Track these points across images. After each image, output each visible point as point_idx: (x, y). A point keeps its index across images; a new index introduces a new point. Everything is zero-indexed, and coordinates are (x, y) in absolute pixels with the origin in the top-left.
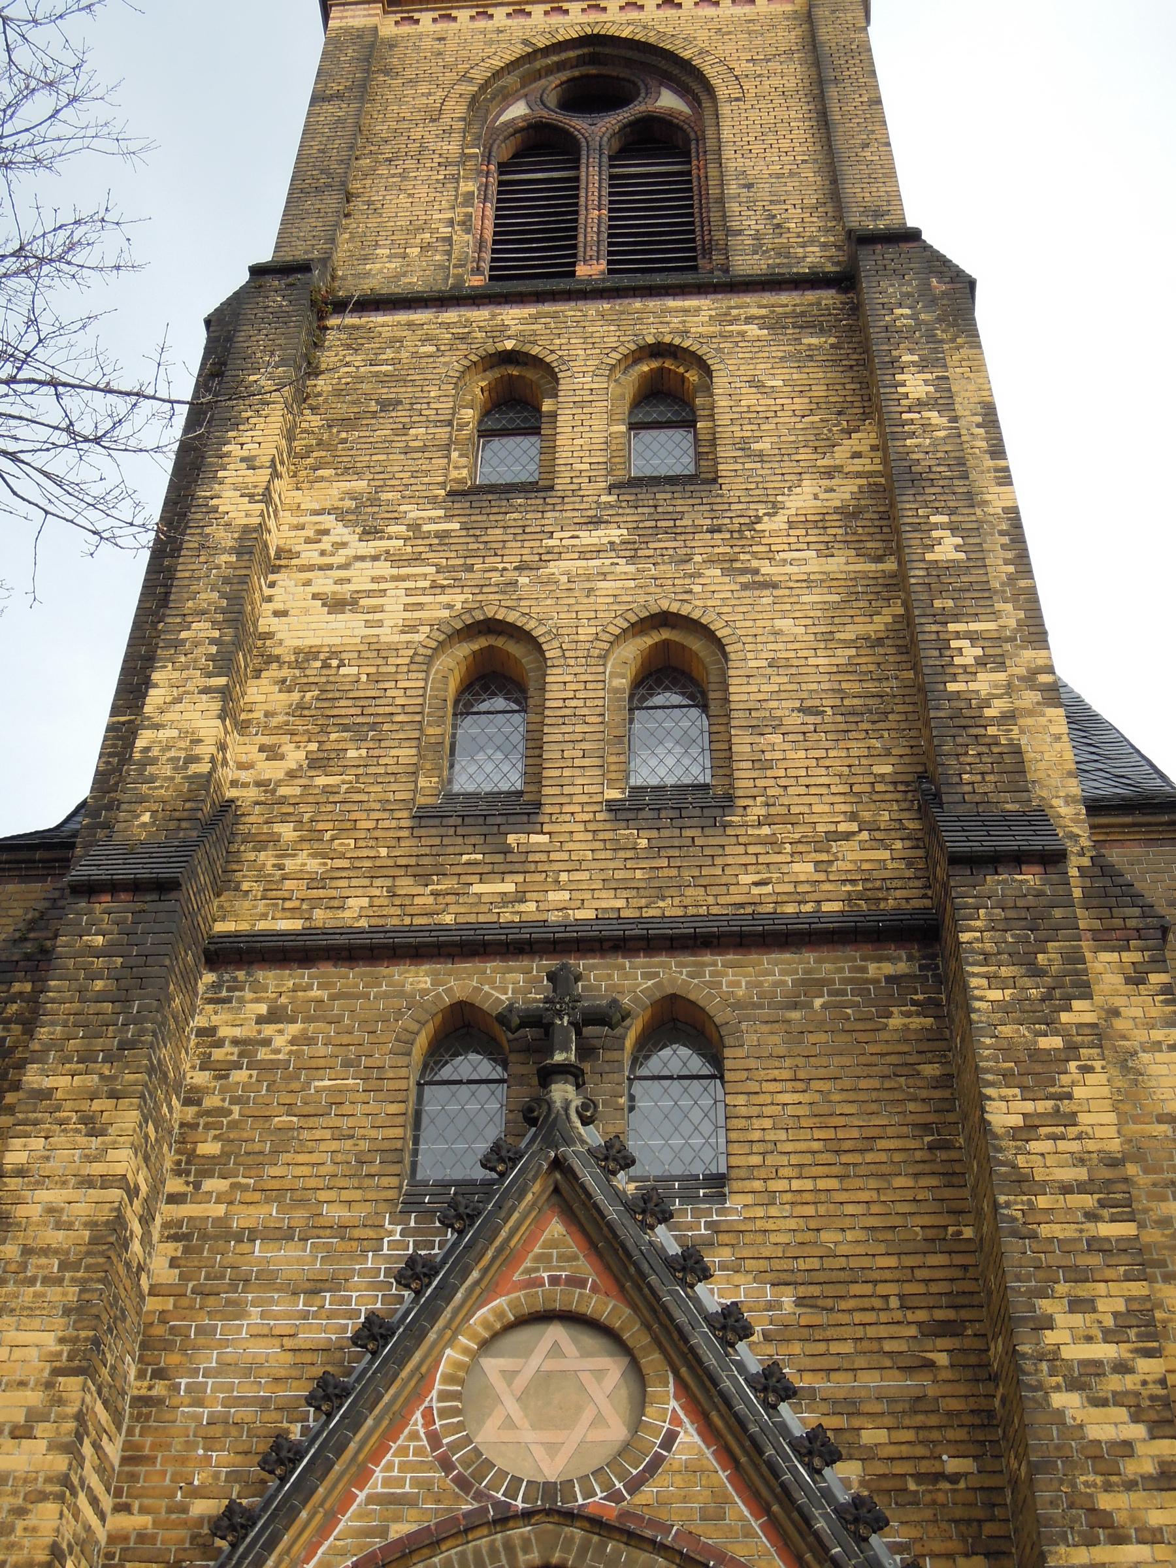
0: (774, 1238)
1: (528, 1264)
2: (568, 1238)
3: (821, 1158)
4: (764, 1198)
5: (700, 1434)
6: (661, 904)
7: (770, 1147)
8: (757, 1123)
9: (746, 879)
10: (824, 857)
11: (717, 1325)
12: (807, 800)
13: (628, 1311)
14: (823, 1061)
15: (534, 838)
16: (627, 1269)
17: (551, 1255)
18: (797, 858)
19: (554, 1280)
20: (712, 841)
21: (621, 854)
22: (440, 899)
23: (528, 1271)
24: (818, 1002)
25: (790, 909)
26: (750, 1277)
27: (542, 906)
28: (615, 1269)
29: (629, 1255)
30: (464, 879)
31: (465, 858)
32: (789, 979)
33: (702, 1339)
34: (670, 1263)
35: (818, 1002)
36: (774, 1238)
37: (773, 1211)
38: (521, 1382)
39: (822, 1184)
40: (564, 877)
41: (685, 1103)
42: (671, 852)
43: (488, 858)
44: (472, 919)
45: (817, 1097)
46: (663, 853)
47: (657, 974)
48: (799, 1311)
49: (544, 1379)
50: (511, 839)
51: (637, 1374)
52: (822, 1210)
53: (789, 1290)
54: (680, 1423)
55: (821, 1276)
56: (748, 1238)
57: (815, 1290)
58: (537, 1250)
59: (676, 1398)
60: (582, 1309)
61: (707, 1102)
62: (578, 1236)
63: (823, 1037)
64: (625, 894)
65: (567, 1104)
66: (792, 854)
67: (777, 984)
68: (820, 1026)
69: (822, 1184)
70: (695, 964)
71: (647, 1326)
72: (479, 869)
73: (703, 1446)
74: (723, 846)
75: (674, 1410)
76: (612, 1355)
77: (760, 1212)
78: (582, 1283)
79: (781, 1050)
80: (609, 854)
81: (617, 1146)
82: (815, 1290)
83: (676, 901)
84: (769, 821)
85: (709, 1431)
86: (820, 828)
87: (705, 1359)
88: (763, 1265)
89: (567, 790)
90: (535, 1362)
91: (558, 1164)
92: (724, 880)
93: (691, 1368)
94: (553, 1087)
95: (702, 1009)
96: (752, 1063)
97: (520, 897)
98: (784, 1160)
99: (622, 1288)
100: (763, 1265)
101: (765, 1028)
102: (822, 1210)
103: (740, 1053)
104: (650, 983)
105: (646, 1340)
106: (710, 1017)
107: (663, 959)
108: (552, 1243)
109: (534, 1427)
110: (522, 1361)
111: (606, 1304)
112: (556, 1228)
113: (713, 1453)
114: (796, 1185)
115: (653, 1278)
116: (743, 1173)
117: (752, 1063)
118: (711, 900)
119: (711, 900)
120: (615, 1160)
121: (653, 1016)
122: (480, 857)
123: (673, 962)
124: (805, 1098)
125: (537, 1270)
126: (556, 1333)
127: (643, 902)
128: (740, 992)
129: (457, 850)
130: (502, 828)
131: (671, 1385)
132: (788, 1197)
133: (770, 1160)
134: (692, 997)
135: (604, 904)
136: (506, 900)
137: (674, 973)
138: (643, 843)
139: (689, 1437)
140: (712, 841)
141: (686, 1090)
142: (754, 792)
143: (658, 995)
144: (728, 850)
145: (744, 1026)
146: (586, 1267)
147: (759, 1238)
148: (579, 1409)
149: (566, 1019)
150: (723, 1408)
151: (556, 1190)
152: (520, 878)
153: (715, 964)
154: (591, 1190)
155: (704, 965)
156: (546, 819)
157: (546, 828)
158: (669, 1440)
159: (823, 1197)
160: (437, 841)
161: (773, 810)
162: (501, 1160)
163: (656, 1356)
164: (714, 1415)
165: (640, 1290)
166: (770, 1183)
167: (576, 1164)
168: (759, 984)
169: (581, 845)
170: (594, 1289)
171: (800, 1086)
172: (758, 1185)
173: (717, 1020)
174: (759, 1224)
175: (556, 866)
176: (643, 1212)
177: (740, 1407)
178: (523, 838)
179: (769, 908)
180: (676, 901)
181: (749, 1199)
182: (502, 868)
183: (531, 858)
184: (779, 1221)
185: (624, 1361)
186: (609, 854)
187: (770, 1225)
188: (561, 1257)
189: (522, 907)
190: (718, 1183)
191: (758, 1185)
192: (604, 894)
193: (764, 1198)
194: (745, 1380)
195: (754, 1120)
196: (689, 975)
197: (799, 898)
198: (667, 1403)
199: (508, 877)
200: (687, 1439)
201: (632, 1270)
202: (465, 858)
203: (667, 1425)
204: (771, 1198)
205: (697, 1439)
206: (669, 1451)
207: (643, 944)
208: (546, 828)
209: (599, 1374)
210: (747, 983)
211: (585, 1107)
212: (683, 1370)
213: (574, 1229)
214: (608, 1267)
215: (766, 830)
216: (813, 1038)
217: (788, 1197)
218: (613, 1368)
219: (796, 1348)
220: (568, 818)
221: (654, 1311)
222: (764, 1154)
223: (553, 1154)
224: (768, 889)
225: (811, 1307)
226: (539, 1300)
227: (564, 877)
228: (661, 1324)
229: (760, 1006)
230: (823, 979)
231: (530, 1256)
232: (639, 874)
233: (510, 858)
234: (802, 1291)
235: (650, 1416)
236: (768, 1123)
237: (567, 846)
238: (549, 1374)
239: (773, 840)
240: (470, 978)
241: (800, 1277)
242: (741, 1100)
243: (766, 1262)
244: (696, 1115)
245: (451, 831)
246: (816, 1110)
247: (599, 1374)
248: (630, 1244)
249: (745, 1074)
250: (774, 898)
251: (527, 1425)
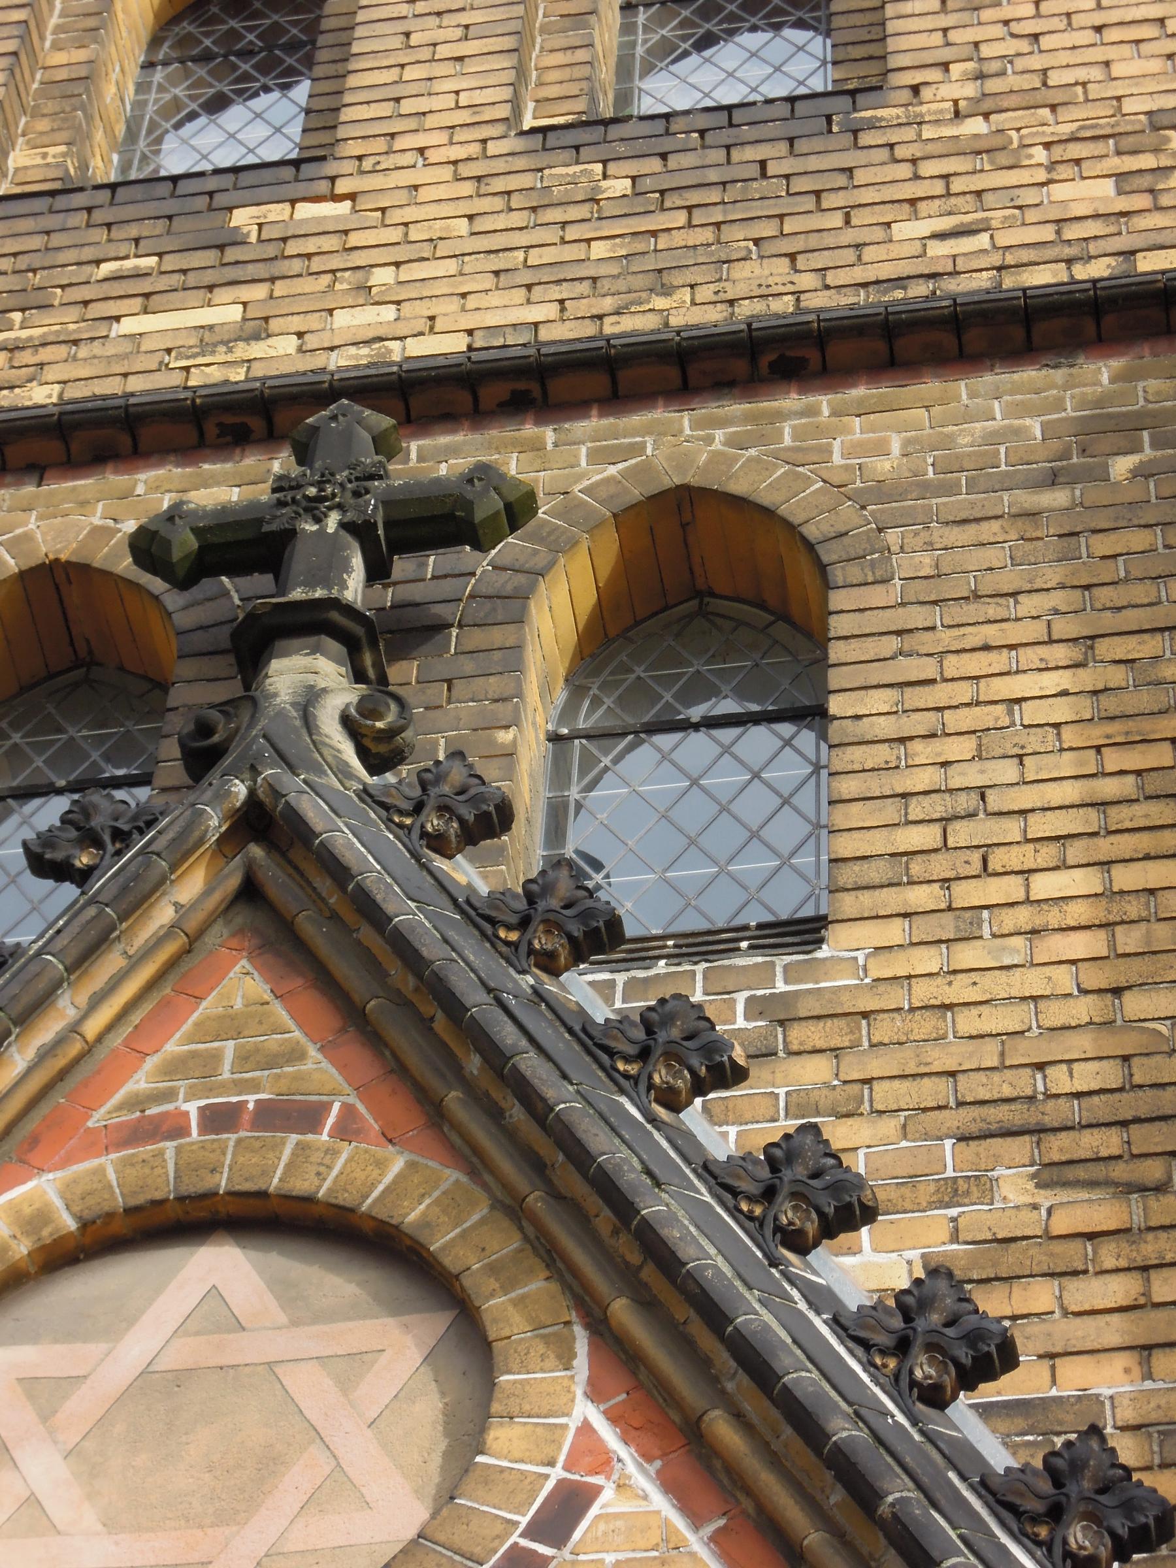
0: (968, 1022)
1: (140, 1082)
2: (280, 1012)
3: (1121, 816)
4: (946, 927)
5: (669, 1486)
6: (660, 303)
7: (965, 802)
8: (922, 751)
9: (909, 230)
10: (1147, 161)
11: (745, 1185)
12: (1099, 54)
13: (452, 1176)
14: (1140, 592)
15: (305, 210)
16: (457, 1069)
17: (215, 1058)
18: (1064, 171)
19: (219, 1119)
20: (814, 163)
21: (556, 215)
22: (26, 357)
23: (137, 1102)
24: (1121, 466)
25: (1041, 277)
26: (890, 1126)
27: (311, 341)
28: (413, 1061)
29: (453, 1006)
30: (96, 310)
31: (106, 268)
32: (1035, 427)
33: (709, 1242)
34: (595, 1042)
35: (1121, 466)
36: (968, 1022)
37: (968, 955)
38: (82, 1407)
39: (1126, 878)
40: (382, 277)
41: (726, 779)
42: (694, 197)
43: (170, 262)
44: (111, 387)
45: (1117, 676)
46: (671, 200)
47: (639, 449)
48: (1046, 1199)
49: (160, 1387)
50: (242, 218)
51: (472, 1347)
52: (1129, 939)
53: (1021, 1147)
54: (604, 1462)
55: (1127, 1106)
56: (884, 1029)
57: (1110, 1142)
58: (173, 1047)
59: (595, 1393)
60: (301, 1185)
61: (790, 771)
62: (313, 1001)
63: (1138, 540)
64: (556, 292)
65: (309, 700)
66: (1052, 166)
67: (994, 438)
68: (1127, 515)
69: (1126, 878)
70: (748, 418)
71: (512, 1209)
72: (146, 286)
73: (679, 1522)
74: (849, 171)
75: (586, 1428)
76: (395, 1309)
77: (928, 960)
78: (307, 1117)
79: (1008, 580)
80: (517, 219)
81: (457, 775)
82: (1110, 1142)
83: (705, 293)
84: (987, 105)
85: (699, 1468)
86: (1129, 106)
87: (686, 1252)
88: (933, 1091)
89: (407, 106)
90: (137, 1348)
91: (262, 822)
92: (849, 236)
93: (647, 1303)
94: (275, 665)
95: (768, 513)
96: (917, 617)
97: (257, 328)
98: (1012, 829)
99: (435, 1114)
100: (933, 1091)
101: (956, 535)
102: (1129, 939)
103: (877, 596)
104: (612, 470)
105: (505, 1243)
106: (791, 528)
107: (659, 414)
108: (228, 1026)
109: (111, 1525)
110: (95, 1349)
111: (381, 1165)
112: (242, 984)
113: (715, 1539)
114: (1045, 886)
115: (530, 1064)
116: (874, 872)
117: (917, 617)
118: (807, 281)
119: (807, 281)
120: (444, 809)
121: (627, 565)
122: (153, 261)
123: (686, 419)
124: (1087, 679)
125: (169, 1095)
126: (221, 1268)
127: (608, 304)
128: (883, 466)
129: (88, 253)
130: (220, 200)
131: (581, 1362)
132: (1023, 917)
133: (961, 834)
134: (738, 487)
135: (492, 319)
136: (208, 339)
137: (688, 442)
138: (622, 186)
139: (635, 1497)
140: (814, 163)
141: (726, 750)
142: (945, 54)
143: (636, 493)
144: (861, 177)
145: (893, 537)
146: (320, 1069)
147: (925, 1025)
148: (270, 1465)
149: (332, 521)
150: (754, 1405)
151: (250, 892)
152: (258, 292)
153: (812, 411)
154: (348, 858)
155: (781, 416)
156: (348, 167)
157: (342, 187)
158: (564, 1511)
159: (1133, 908)
160: (37, 242)
161: (993, 85)
162: (91, 839)
163: (538, 1285)
164: (722, 1429)
165: (495, 1114)
166: (958, 888)
167: (313, 810)
168: (947, 442)
169: (440, 204)
170: (347, 1130)
171: (1060, 654)
172: (922, 897)
173: (811, 532)
174: (923, 992)
175: (359, 259)
176: (524, 923)
177: (802, 1377)
178: (277, 212)
179: (983, 281)
180: (705, 293)
181: (895, 932)
182: (209, 277)
183: (292, 248)
184: (986, 980)
185: (435, 1324)
186: (517, 219)
187: (960, 990)
188: (244, 1059)
189: (257, 350)
190: (805, 932)
191: (922, 897)
192: (495, 299)
193: (946, 927)
194: (837, 1323)
195: (917, 746)
196: (730, 442)
197: (1068, 252)
198: (562, 1407)
199: (222, 295)
200: (626, 1506)
201: (474, 1064)
202: (106, 268)
203: (557, 1473)
204: (967, 923)
205: (661, 1503)
206: (559, 1538)
207: (598, 382)
208: (342, 187)
209: (349, 1368)
210: (907, 443)
211: (368, 709)
212: (621, 1310)
213: (296, 983)
214: (399, 1069)
215: (976, 126)
216: (1103, 545)
217: (1023, 917)
218: (396, 1349)
219: (1040, 1296)
220: (409, 158)
221: (538, 1167)
222: (945, 821)
223: (240, 790)
224: (983, 240)
225: (1092, 1184)
226: (163, 1170)
227: (382, 277)
228: (557, 1196)
229: (950, 489)
230: (1138, 415)
231: (151, 1063)
232: (599, 250)
233: (231, 254)
234: (1059, 1147)
235: (506, 1446)
236: (960, 748)
237: (395, 216)
238: (180, 1378)
239: (998, 141)
240: (84, 505)
241: (1054, 1113)
242: (880, 701)
243: (944, 1084)
244: (755, 805)
245: (80, 218)
246: (1110, 704)
247: (349, 1368)
248: (475, 999)
249: (894, 643)
250: (996, 259)
251: (90, 1518)
